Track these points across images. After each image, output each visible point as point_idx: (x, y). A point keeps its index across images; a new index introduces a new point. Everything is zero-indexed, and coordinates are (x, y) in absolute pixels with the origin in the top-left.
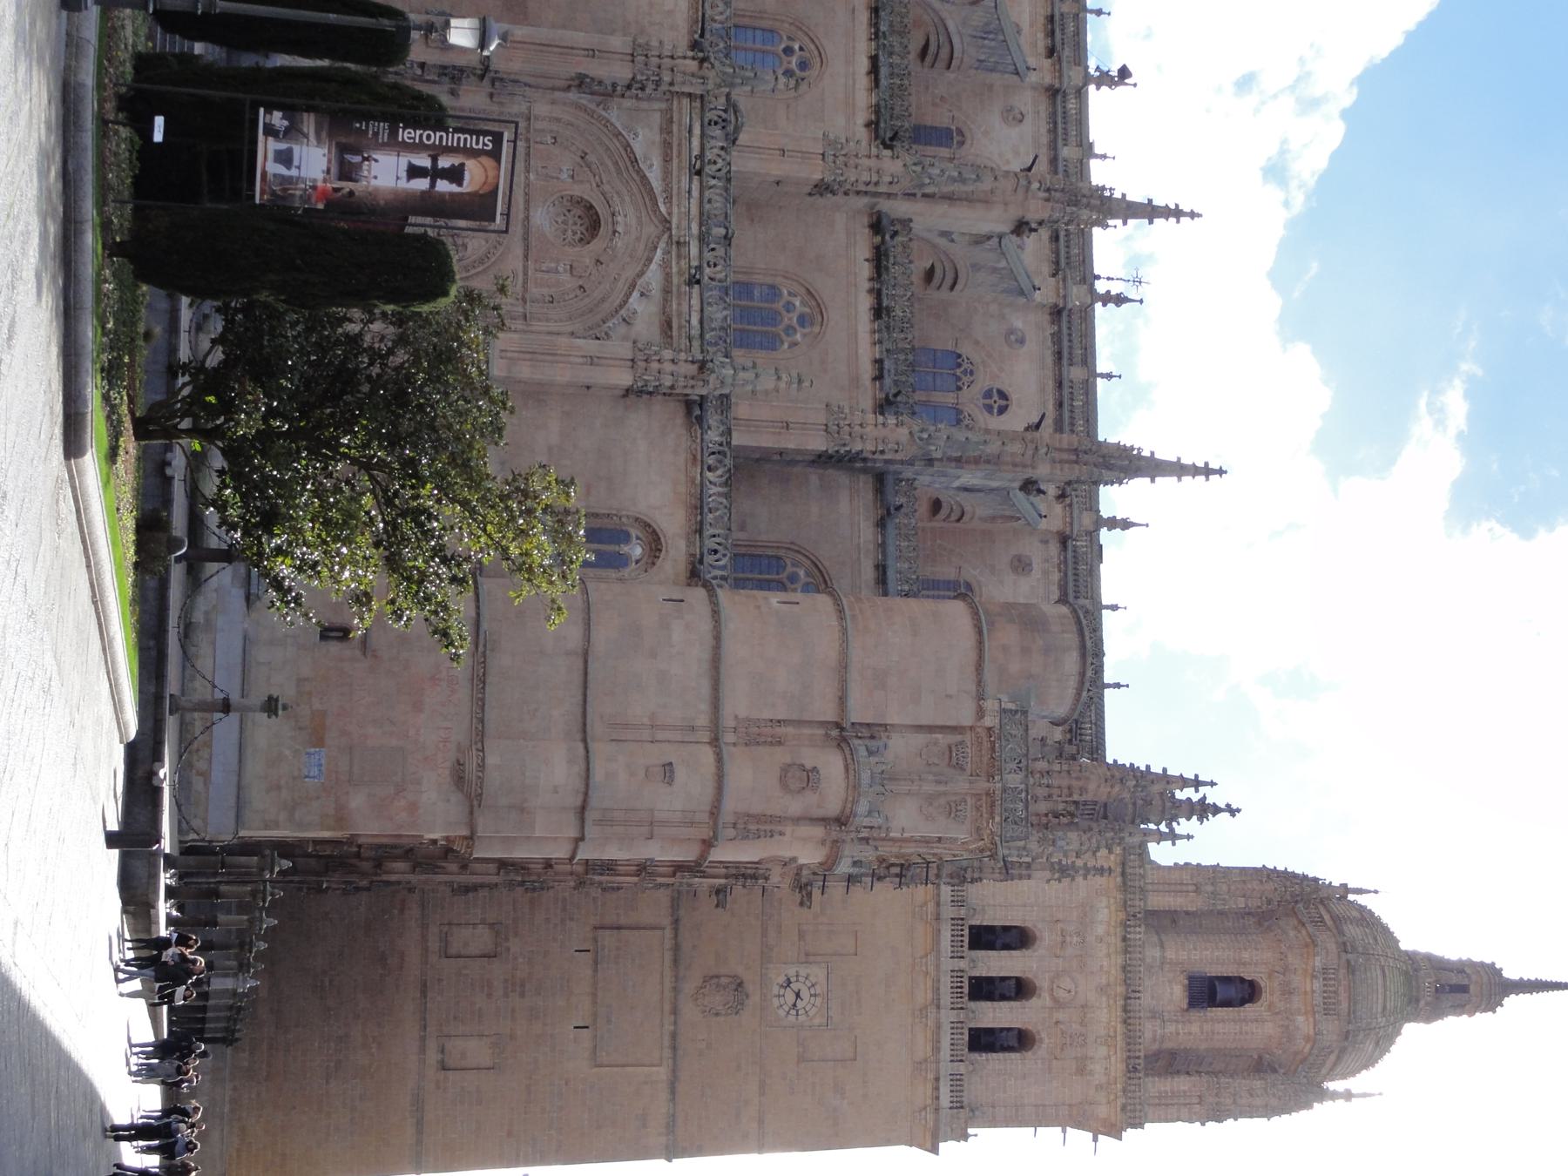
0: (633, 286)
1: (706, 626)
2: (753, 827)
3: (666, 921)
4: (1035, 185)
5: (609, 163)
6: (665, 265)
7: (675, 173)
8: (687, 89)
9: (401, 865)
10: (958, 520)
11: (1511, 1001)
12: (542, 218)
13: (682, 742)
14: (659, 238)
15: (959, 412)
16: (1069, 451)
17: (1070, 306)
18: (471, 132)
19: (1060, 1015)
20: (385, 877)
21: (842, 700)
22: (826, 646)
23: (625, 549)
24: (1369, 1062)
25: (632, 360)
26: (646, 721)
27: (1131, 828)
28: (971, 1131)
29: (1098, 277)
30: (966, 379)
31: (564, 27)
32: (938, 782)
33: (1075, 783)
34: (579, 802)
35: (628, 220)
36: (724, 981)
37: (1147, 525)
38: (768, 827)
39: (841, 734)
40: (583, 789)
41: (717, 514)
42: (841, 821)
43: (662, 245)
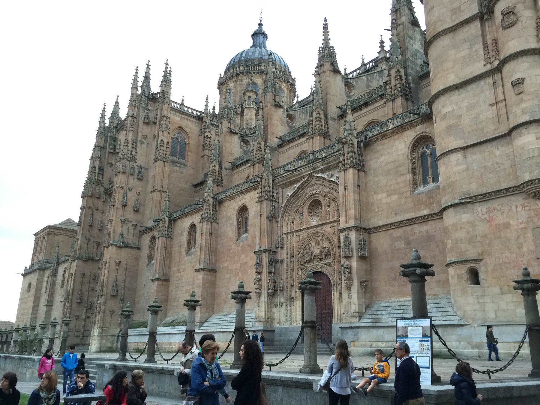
1: (442, 99)
6: (323, 171)
7: (296, 178)
8: (271, 181)
12: (314, 222)
13: (503, 86)
14: (315, 176)
23: (428, 152)
41: (405, 118)
43: (316, 175)
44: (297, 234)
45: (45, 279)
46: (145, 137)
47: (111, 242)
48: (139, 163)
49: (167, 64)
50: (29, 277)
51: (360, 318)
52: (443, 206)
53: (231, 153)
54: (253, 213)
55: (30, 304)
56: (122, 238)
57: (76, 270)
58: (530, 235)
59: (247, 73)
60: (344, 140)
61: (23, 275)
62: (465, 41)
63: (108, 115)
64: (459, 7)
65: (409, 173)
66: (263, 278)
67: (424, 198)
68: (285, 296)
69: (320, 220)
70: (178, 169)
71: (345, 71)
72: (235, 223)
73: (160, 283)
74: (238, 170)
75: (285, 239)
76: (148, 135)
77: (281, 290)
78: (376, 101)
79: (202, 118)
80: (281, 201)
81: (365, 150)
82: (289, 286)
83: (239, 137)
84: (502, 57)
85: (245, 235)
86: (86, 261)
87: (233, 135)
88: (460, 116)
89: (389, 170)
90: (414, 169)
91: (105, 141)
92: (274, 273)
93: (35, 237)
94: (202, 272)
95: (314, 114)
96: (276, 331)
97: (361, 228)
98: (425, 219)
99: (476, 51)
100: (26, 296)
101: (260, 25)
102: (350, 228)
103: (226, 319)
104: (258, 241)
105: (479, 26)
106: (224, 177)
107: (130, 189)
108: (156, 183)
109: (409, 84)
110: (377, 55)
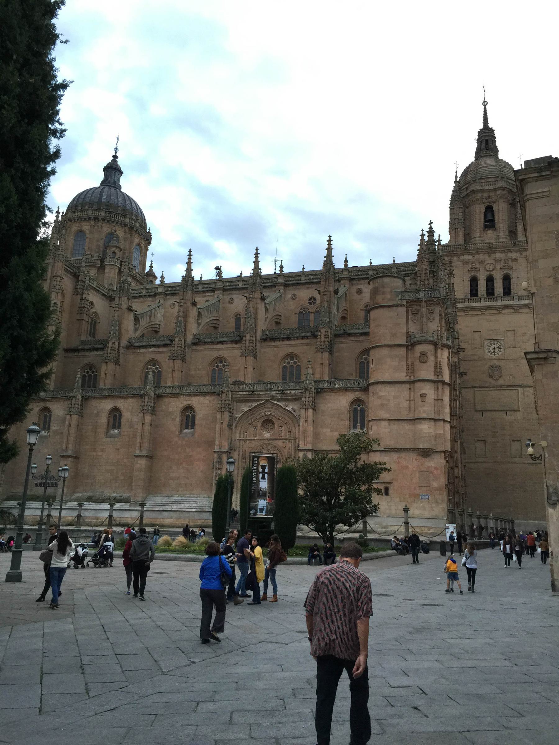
1: (380, 387)
2: (438, 370)
3: (472, 390)
4: (251, 296)
5: (251, 417)
6: (279, 400)
9: (456, 471)
10: (347, 311)
12: (267, 435)
15: (316, 311)
16: (326, 282)
17: (284, 281)
18: (253, 464)
20: (460, 475)
22: (385, 351)
23: (359, 409)
25: (306, 409)
27: (437, 254)
29: (275, 272)
30: (306, 310)
31: (215, 431)
32: (423, 317)
33: (424, 272)
35: (267, 411)
37: (346, 255)
38: (438, 366)
39: (410, 345)
42: (435, 344)
43: (273, 401)
58: (417, 474)
59: (108, 221)
69: (272, 435)
72: (178, 419)
73: (73, 460)
75: (238, 443)
78: (298, 339)
90: (350, 417)
94: (144, 459)
99: (402, 365)
101: (115, 157)
106: (121, 356)
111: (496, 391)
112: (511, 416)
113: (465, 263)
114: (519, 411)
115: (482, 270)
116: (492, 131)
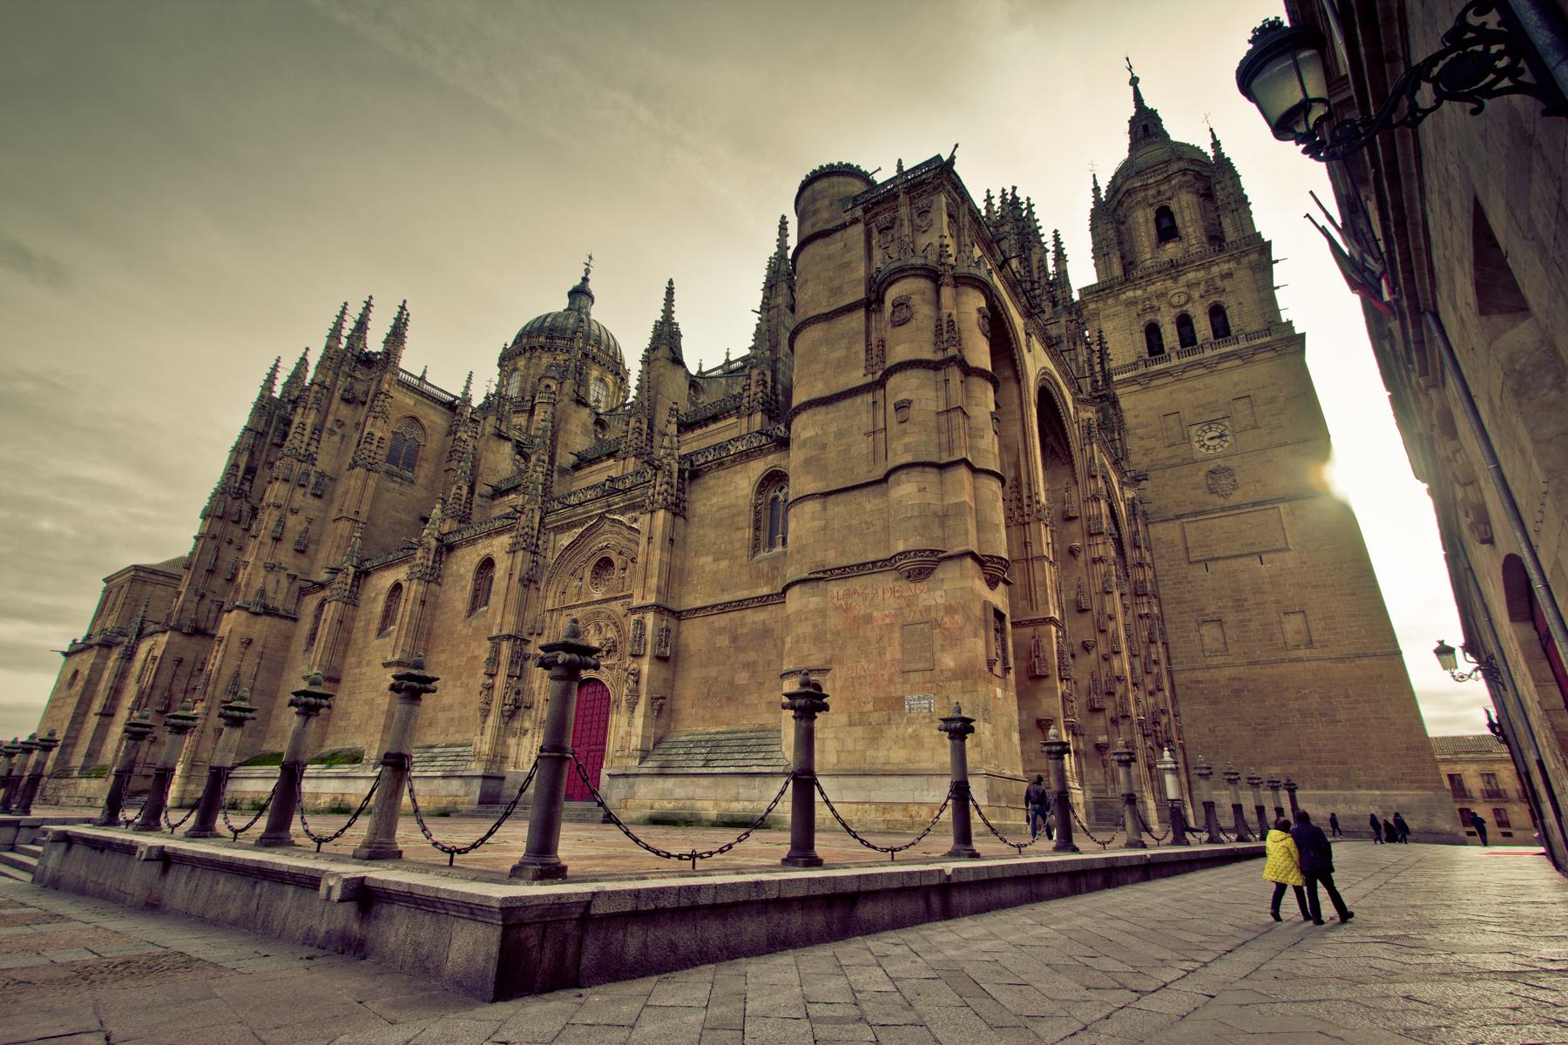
0: (631, 528)
2: (946, 336)
3: (1178, 522)
6: (623, 511)
8: (537, 520)
9: (1116, 662)
11: (1149, 103)
12: (598, 596)
19: (1196, 295)
20: (1128, 674)
21: (849, 309)
23: (781, 498)
24: (1198, 149)
26: (870, 439)
28: (1284, 320)
34: (935, 471)
36: (1210, 482)
38: (945, 326)
39: (872, 302)
40: (920, 469)
43: (612, 516)
44: (568, 612)
45: (110, 664)
46: (340, 423)
47: (237, 603)
48: (320, 466)
49: (403, 308)
50: (77, 658)
51: (643, 759)
52: (788, 581)
53: (494, 471)
54: (502, 571)
55: (69, 710)
56: (261, 597)
57: (164, 651)
58: (897, 635)
59: (549, 349)
60: (657, 462)
61: (66, 654)
62: (842, 336)
63: (282, 377)
64: (841, 287)
65: (749, 527)
66: (497, 684)
67: (765, 567)
68: (533, 718)
70: (397, 486)
71: (700, 367)
74: (502, 500)
76: (348, 422)
77: (526, 707)
79: (457, 407)
80: (549, 554)
81: (690, 484)
82: (542, 701)
83: (513, 446)
84: (889, 364)
85: (485, 608)
86: (188, 635)
87: (502, 441)
88: (824, 446)
89: (721, 519)
90: (757, 522)
91: (269, 423)
92: (519, 678)
93: (105, 585)
95: (632, 421)
96: (508, 778)
97: (665, 609)
98: (763, 601)
99: (856, 353)
100: (63, 694)
101: (585, 280)
102: (647, 607)
103: (426, 755)
104: (499, 620)
105: (863, 318)
107: (295, 512)
108: (346, 505)
109: (776, 396)
110: (748, 352)
111: (1230, 518)
112: (1271, 562)
113: (1131, 303)
114: (1288, 549)
115: (1164, 308)
116: (1153, 113)
